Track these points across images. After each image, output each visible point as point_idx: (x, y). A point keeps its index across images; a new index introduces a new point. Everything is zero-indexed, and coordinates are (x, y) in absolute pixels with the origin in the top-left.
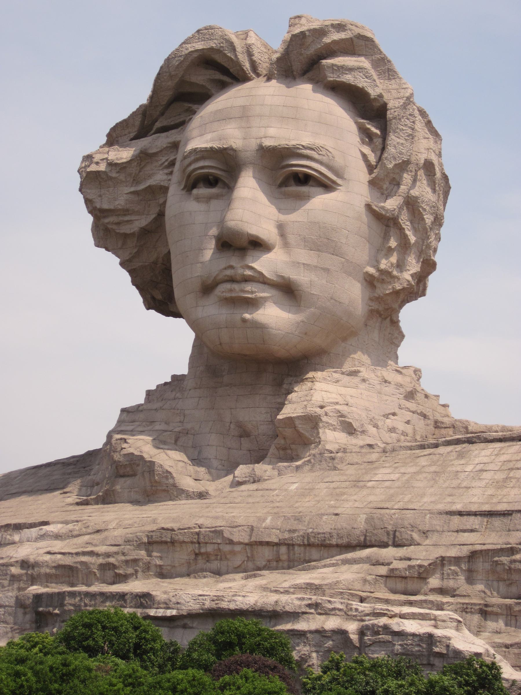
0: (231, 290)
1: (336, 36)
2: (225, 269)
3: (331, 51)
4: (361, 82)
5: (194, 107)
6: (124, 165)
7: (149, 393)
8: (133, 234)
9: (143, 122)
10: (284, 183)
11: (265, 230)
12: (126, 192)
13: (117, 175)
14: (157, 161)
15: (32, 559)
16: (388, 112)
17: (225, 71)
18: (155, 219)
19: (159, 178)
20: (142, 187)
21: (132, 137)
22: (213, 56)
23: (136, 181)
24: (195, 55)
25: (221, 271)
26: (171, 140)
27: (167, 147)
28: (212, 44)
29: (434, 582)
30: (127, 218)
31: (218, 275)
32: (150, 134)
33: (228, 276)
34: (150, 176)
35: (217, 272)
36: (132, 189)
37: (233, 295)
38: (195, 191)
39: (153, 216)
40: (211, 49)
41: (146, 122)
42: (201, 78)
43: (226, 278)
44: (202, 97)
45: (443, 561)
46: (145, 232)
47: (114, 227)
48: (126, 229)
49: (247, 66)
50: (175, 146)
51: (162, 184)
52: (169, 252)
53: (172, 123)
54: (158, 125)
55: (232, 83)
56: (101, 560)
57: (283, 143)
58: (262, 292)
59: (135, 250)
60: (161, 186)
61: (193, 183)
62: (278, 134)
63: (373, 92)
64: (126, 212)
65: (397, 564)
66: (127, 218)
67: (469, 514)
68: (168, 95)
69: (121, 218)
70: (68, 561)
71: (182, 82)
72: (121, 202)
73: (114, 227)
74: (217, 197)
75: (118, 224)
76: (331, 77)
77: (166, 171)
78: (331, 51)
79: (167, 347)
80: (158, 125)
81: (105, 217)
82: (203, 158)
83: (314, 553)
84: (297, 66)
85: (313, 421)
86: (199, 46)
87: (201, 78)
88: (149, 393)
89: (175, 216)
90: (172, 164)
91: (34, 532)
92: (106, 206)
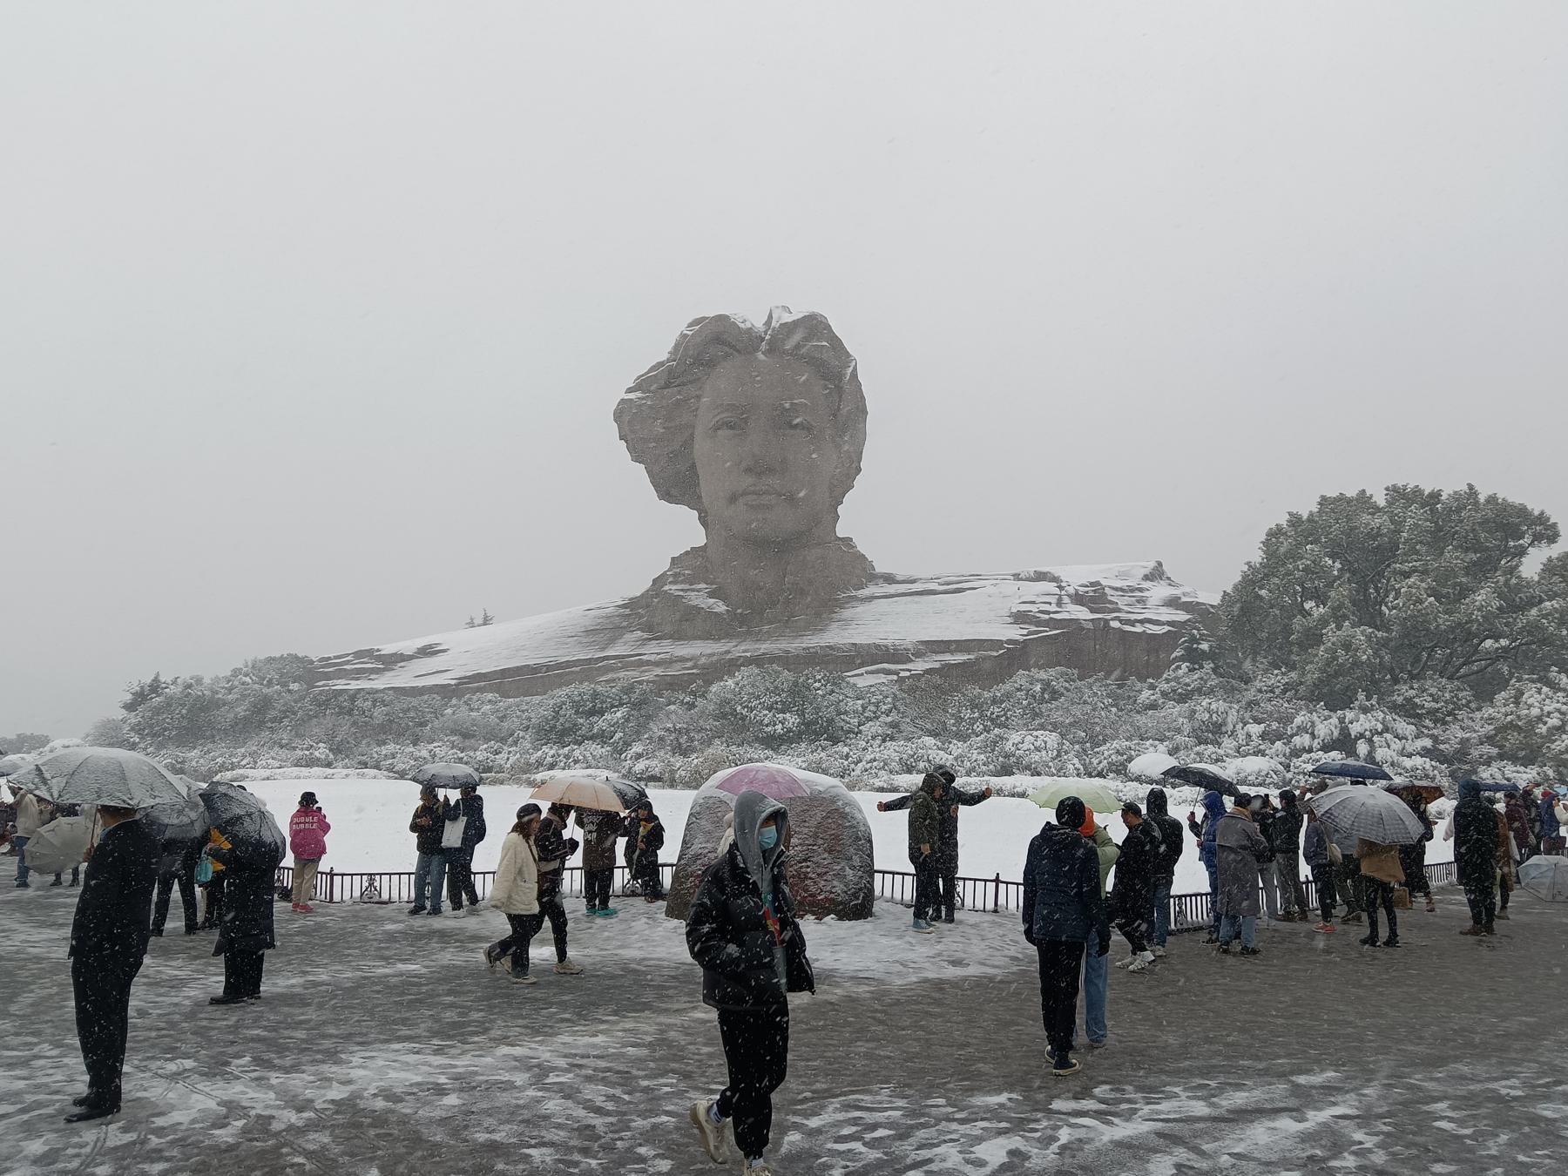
17: (732, 347)
44: (711, 364)
50: (699, 397)
79: (683, 529)
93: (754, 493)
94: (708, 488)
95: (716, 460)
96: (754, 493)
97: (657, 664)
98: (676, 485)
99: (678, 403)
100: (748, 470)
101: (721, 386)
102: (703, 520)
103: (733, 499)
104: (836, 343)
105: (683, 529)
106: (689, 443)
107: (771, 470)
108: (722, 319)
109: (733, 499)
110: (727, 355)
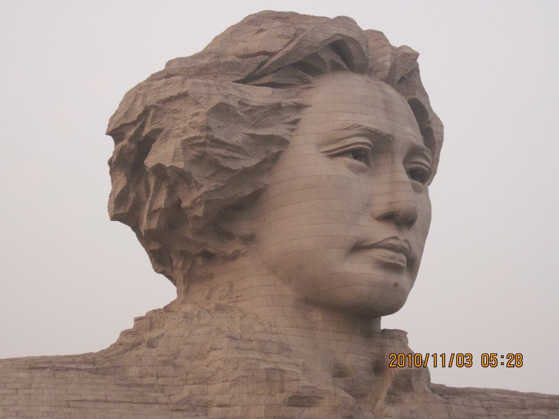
0: (392, 258)
2: (390, 238)
5: (309, 77)
6: (254, 108)
8: (235, 171)
9: (255, 71)
12: (245, 132)
13: (243, 114)
14: (279, 114)
16: (435, 135)
18: (259, 164)
19: (279, 130)
20: (261, 132)
21: (236, 79)
22: (349, 44)
23: (256, 126)
24: (339, 38)
25: (387, 239)
26: (297, 100)
27: (292, 105)
28: (351, 34)
30: (236, 155)
31: (381, 242)
32: (252, 83)
33: (391, 244)
34: (270, 125)
35: (381, 239)
36: (251, 131)
37: (393, 261)
39: (259, 161)
40: (351, 39)
41: (257, 72)
42: (328, 57)
43: (390, 246)
46: (246, 172)
47: (220, 159)
50: (299, 107)
51: (285, 137)
53: (280, 82)
54: (268, 79)
55: (347, 71)
59: (223, 185)
60: (284, 138)
64: (237, 149)
66: (236, 155)
69: (231, 154)
72: (237, 139)
73: (220, 159)
74: (363, 170)
75: (225, 157)
77: (289, 127)
80: (268, 79)
81: (212, 146)
82: (364, 135)
84: (398, 77)
86: (344, 32)
89: (329, 176)
90: (295, 122)
92: (223, 139)
93: (393, 248)
96: (393, 248)
99: (277, 108)
103: (358, 247)
109: (358, 247)
110: (336, 68)
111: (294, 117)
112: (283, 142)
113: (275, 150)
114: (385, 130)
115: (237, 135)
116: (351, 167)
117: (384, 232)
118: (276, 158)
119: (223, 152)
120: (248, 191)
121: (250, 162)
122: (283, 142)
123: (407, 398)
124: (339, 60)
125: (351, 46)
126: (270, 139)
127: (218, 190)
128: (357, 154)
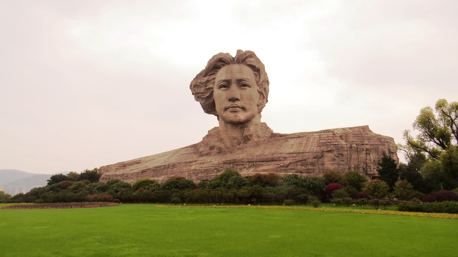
1: (248, 54)
3: (247, 58)
4: (254, 64)
7: (209, 131)
10: (241, 86)
11: (238, 97)
15: (197, 169)
17: (224, 62)
19: (211, 86)
20: (207, 87)
29: (290, 167)
38: (221, 89)
45: (290, 163)
46: (208, 97)
48: (202, 97)
49: (230, 61)
50: (214, 79)
52: (214, 101)
56: (214, 168)
57: (241, 78)
58: (238, 109)
61: (220, 87)
62: (239, 76)
63: (257, 66)
65: (281, 164)
67: (294, 153)
68: (212, 67)
70: (206, 169)
71: (215, 65)
74: (226, 90)
76: (248, 63)
78: (247, 58)
83: (261, 163)
84: (241, 61)
85: (251, 136)
87: (219, 64)
88: (209, 131)
90: (214, 82)
91: (194, 163)
93: (232, 107)
94: (218, 108)
95: (220, 96)
96: (232, 107)
97: (200, 164)
98: (210, 108)
99: (208, 81)
100: (230, 100)
101: (221, 75)
102: (218, 119)
103: (226, 109)
104: (258, 61)
105: (212, 122)
106: (212, 92)
107: (237, 100)
108: (221, 54)
109: (226, 109)
110: (224, 65)
111: (214, 81)
112: (212, 88)
113: (212, 90)
114: (228, 79)
115: (202, 90)
116: (222, 90)
117: (230, 104)
118: (213, 91)
119: (200, 95)
120: (212, 101)
121: (208, 95)
122: (212, 88)
123: (250, 142)
124: (223, 63)
125: (223, 59)
126: (209, 88)
127: (205, 103)
128: (224, 86)
